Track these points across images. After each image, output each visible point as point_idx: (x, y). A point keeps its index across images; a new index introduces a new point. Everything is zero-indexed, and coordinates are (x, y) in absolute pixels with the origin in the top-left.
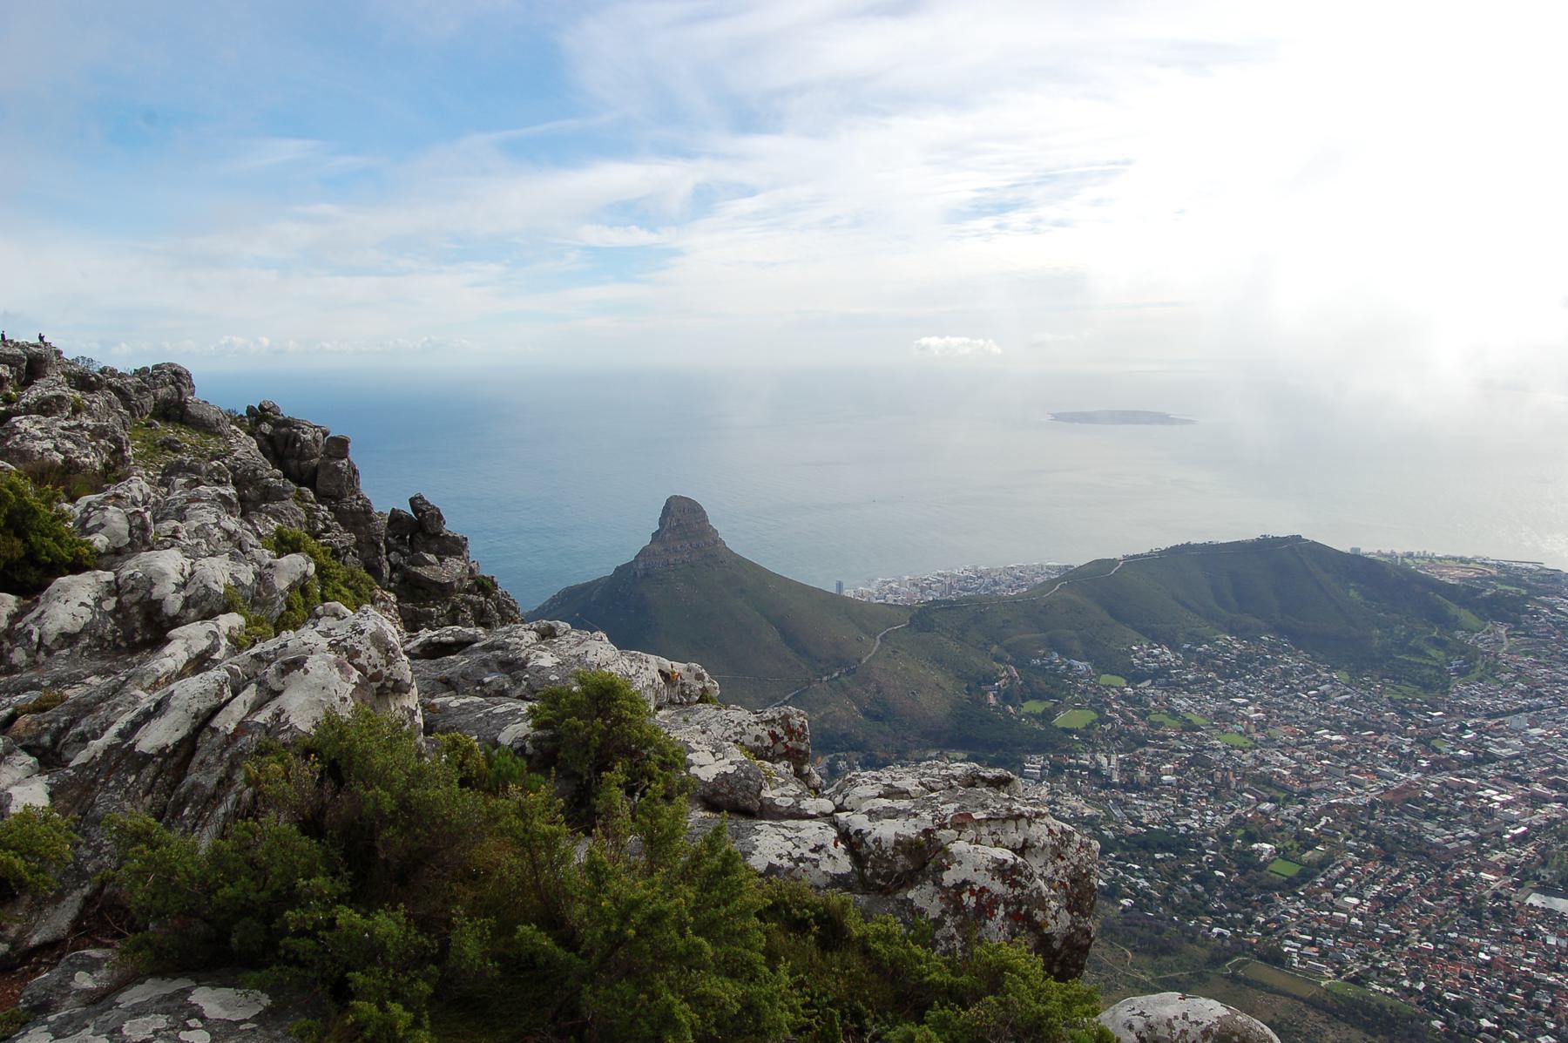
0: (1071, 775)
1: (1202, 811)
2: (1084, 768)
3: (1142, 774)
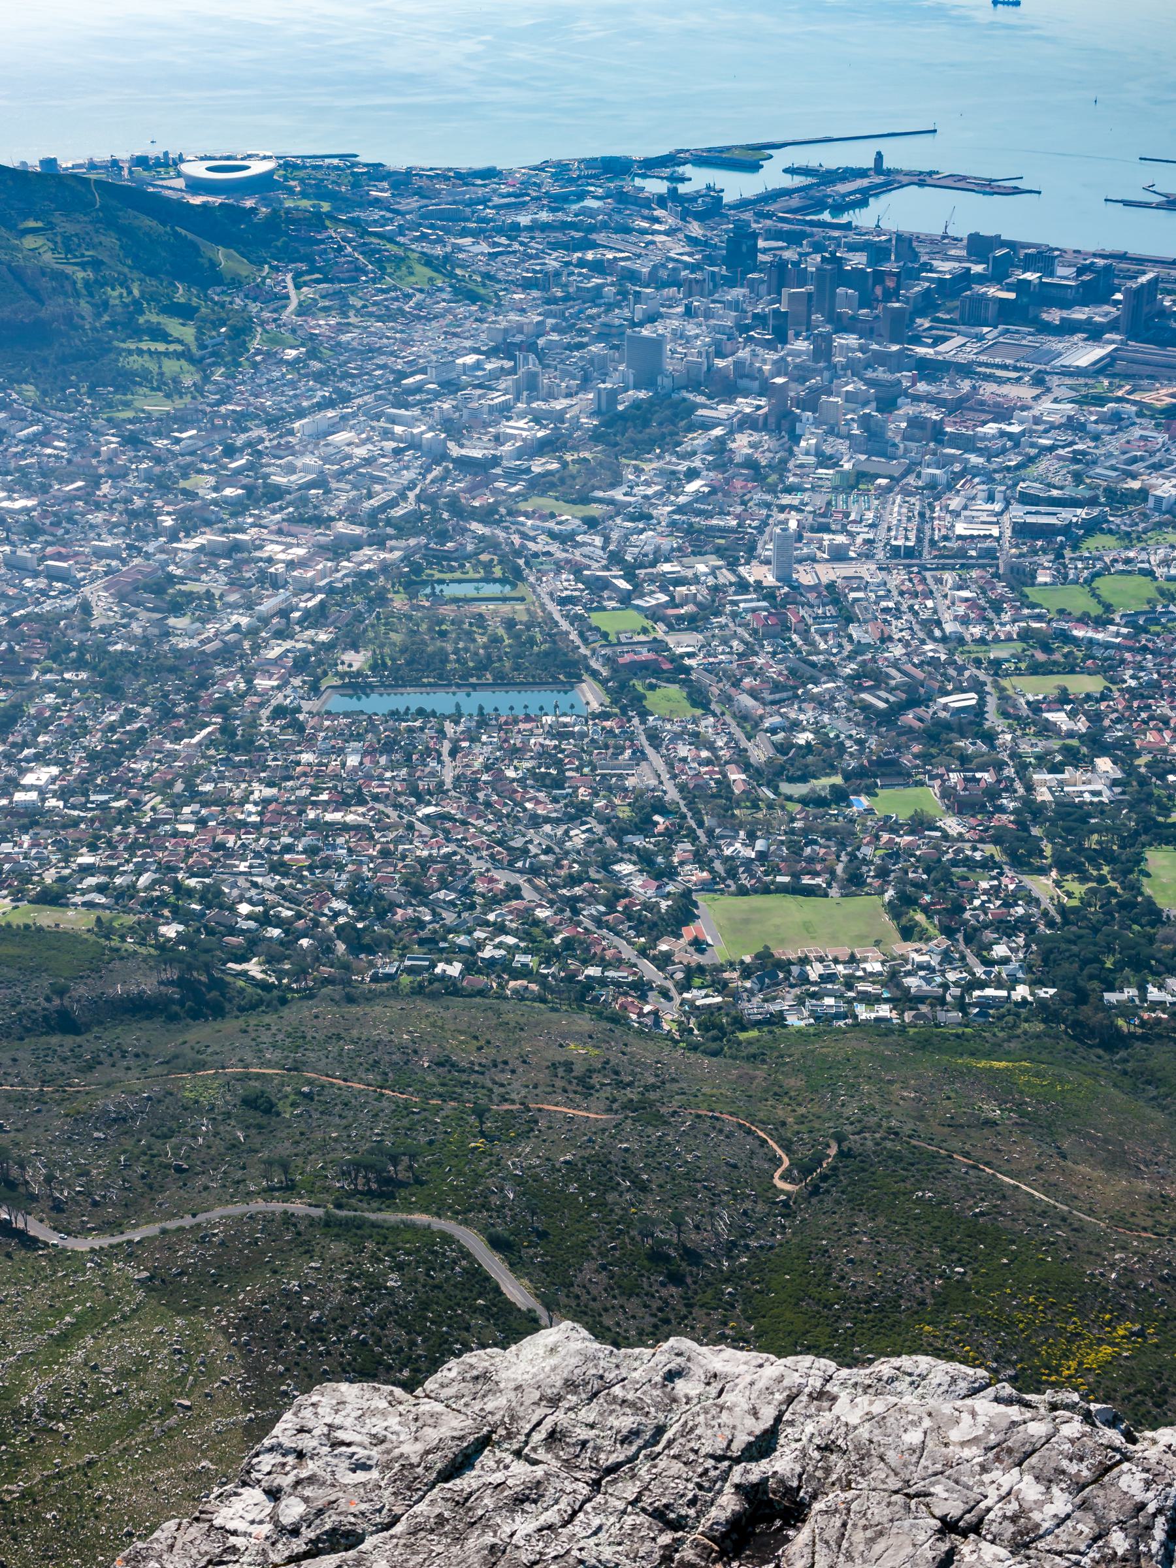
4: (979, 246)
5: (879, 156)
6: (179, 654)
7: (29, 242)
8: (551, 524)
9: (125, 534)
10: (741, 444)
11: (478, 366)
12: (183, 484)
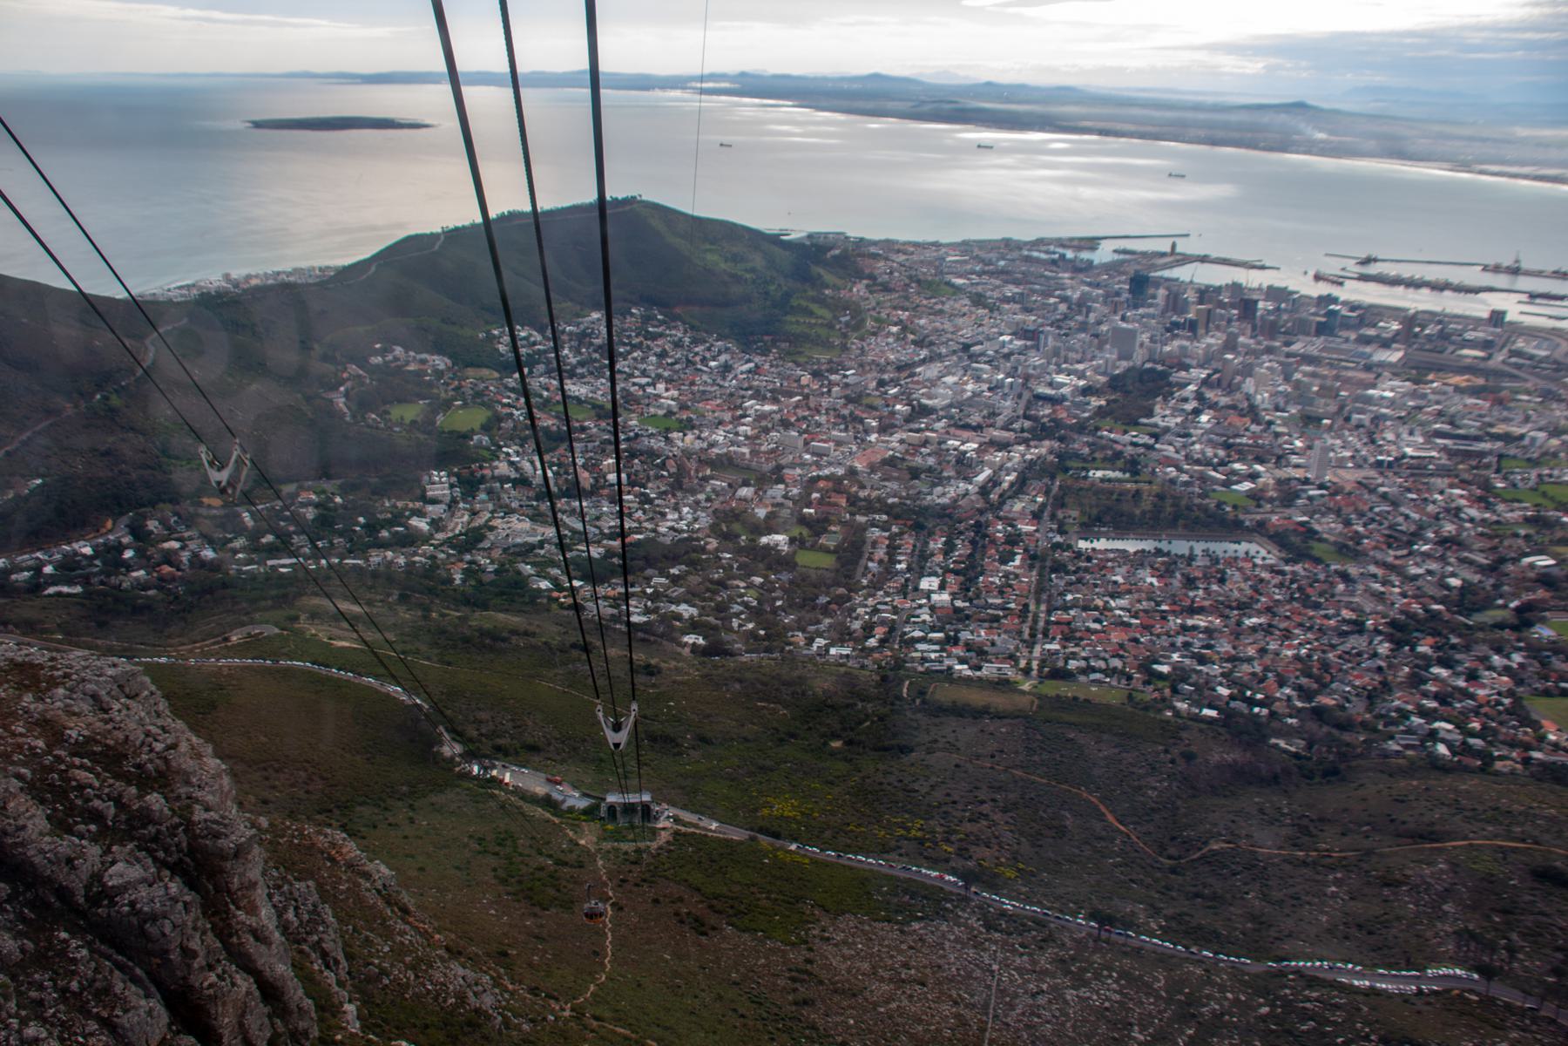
0: (490, 492)
1: (676, 508)
2: (504, 479)
3: (586, 474)
4: (1275, 293)
5: (1174, 246)
6: (944, 507)
7: (709, 257)
8: (1127, 438)
9: (846, 430)
10: (1209, 394)
11: (1011, 342)
12: (865, 401)
